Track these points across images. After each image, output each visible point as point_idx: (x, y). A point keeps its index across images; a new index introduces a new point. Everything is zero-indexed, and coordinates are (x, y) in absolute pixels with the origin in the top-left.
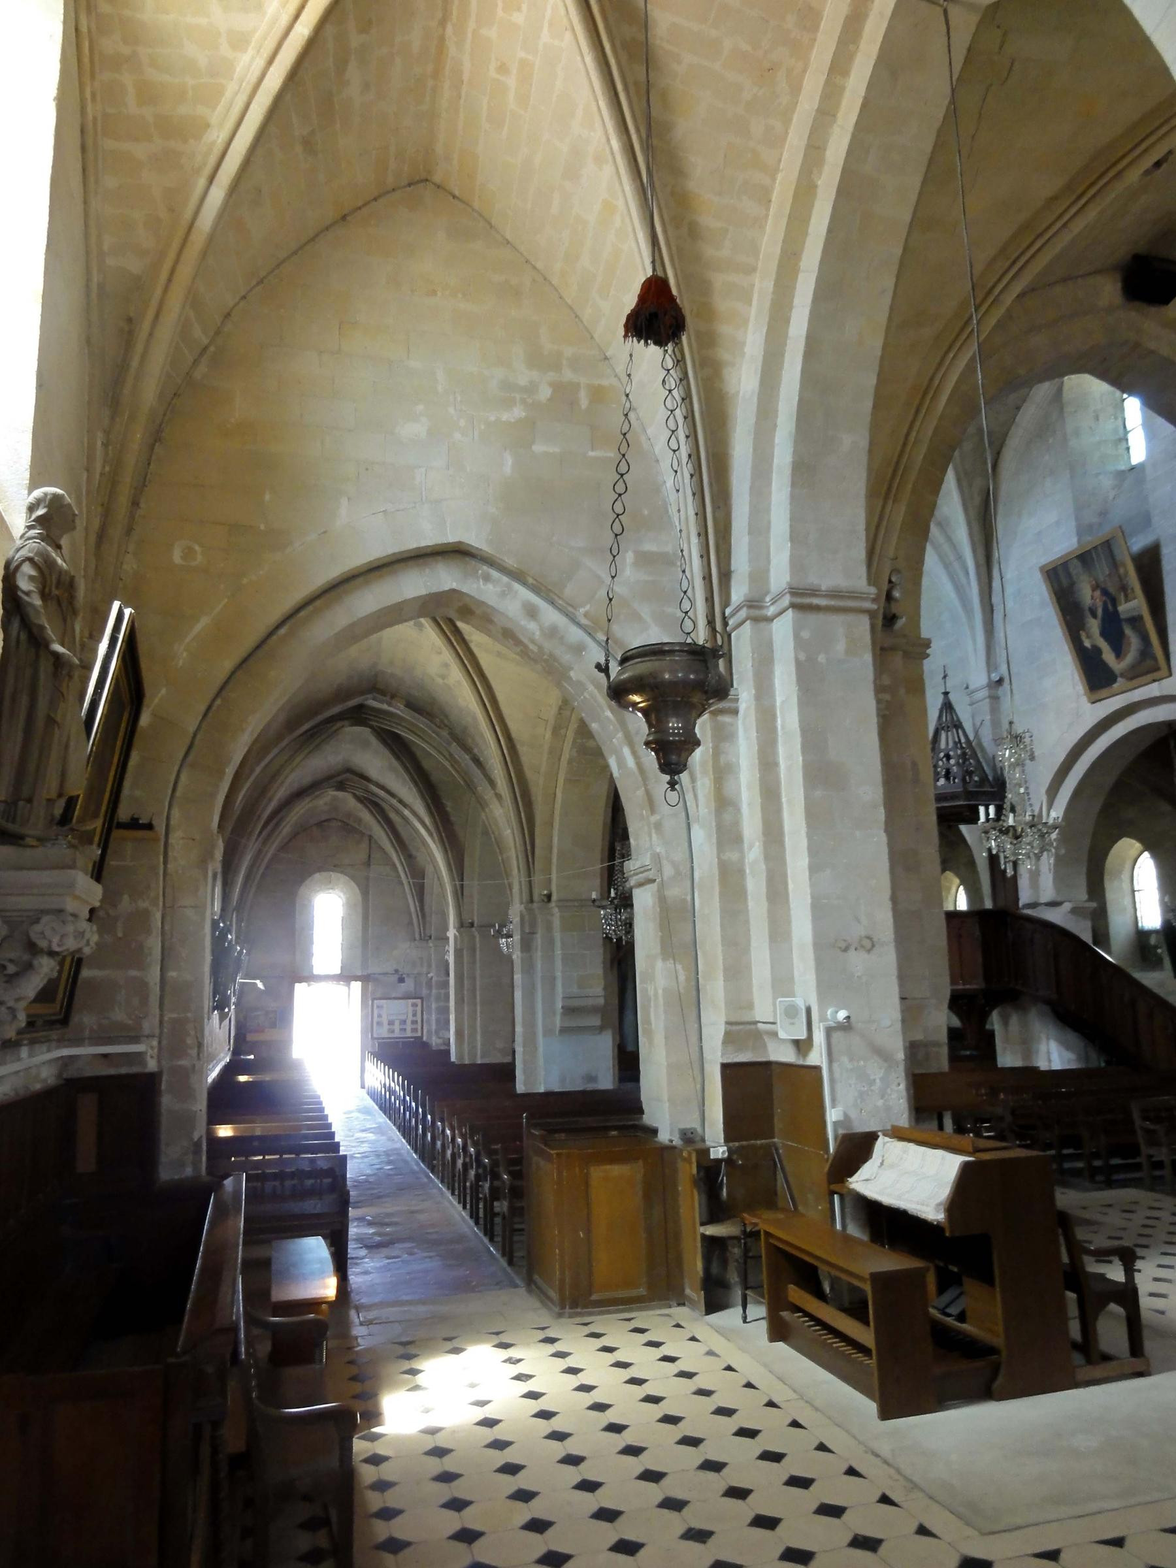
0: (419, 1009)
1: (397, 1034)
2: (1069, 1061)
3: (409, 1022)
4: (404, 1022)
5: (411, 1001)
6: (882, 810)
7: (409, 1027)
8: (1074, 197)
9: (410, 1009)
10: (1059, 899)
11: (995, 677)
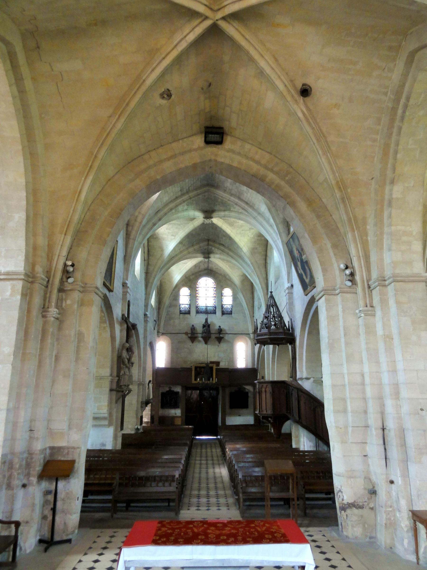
2: (310, 447)
6: (12, 357)
8: (117, 116)
10: (309, 377)
11: (289, 285)
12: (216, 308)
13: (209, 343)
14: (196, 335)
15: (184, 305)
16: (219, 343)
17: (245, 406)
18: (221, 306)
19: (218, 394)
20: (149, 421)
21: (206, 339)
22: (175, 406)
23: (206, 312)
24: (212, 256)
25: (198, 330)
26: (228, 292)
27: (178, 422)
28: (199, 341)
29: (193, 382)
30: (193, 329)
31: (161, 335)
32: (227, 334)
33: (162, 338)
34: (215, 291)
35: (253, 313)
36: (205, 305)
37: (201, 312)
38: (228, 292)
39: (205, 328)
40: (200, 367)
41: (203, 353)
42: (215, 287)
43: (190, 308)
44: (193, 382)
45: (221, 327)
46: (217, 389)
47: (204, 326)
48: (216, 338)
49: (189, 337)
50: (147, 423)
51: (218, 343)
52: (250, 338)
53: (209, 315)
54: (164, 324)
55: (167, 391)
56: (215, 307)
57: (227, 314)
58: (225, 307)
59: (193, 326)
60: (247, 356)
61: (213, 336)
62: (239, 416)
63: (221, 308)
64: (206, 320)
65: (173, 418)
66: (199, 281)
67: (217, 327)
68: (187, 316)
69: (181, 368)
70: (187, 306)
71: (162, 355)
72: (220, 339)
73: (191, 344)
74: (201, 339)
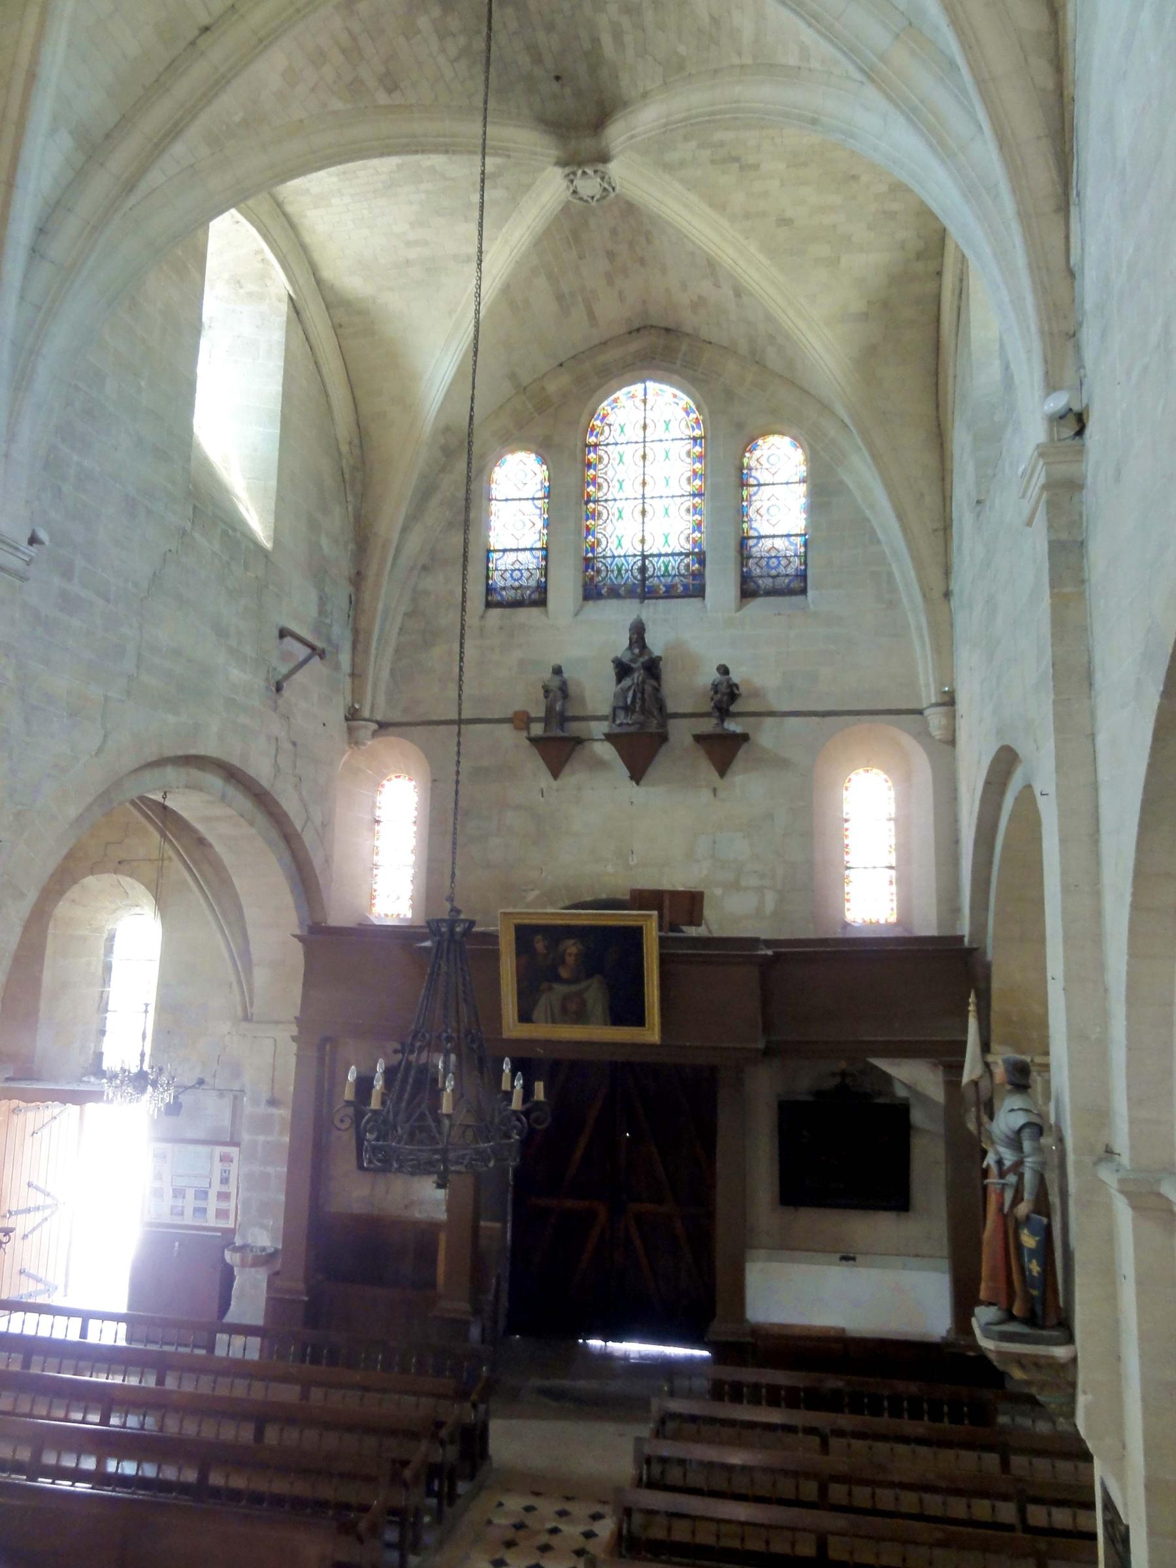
1: (188, 1219)
3: (212, 1195)
4: (202, 1194)
5: (219, 1150)
7: (213, 1204)
9: (218, 1167)
12: (702, 562)
13: (653, 772)
14: (574, 728)
15: (511, 557)
16: (722, 773)
17: (889, 1191)
18: (733, 544)
21: (640, 750)
23: (644, 587)
24: (617, 134)
26: (779, 462)
28: (600, 764)
29: (512, 1027)
31: (375, 734)
32: (771, 714)
33: (390, 747)
35: (947, 572)
37: (614, 593)
38: (779, 462)
39: (627, 682)
40: (556, 934)
41: (621, 835)
42: (698, 433)
44: (512, 1027)
45: (735, 677)
48: (699, 738)
49: (534, 741)
51: (715, 775)
52: (923, 735)
54: (392, 671)
56: (701, 558)
59: (558, 671)
60: (904, 849)
61: (681, 733)
62: (845, 1258)
63: (732, 553)
64: (638, 632)
67: (710, 675)
70: (530, 561)
73: (545, 779)
74: (606, 751)
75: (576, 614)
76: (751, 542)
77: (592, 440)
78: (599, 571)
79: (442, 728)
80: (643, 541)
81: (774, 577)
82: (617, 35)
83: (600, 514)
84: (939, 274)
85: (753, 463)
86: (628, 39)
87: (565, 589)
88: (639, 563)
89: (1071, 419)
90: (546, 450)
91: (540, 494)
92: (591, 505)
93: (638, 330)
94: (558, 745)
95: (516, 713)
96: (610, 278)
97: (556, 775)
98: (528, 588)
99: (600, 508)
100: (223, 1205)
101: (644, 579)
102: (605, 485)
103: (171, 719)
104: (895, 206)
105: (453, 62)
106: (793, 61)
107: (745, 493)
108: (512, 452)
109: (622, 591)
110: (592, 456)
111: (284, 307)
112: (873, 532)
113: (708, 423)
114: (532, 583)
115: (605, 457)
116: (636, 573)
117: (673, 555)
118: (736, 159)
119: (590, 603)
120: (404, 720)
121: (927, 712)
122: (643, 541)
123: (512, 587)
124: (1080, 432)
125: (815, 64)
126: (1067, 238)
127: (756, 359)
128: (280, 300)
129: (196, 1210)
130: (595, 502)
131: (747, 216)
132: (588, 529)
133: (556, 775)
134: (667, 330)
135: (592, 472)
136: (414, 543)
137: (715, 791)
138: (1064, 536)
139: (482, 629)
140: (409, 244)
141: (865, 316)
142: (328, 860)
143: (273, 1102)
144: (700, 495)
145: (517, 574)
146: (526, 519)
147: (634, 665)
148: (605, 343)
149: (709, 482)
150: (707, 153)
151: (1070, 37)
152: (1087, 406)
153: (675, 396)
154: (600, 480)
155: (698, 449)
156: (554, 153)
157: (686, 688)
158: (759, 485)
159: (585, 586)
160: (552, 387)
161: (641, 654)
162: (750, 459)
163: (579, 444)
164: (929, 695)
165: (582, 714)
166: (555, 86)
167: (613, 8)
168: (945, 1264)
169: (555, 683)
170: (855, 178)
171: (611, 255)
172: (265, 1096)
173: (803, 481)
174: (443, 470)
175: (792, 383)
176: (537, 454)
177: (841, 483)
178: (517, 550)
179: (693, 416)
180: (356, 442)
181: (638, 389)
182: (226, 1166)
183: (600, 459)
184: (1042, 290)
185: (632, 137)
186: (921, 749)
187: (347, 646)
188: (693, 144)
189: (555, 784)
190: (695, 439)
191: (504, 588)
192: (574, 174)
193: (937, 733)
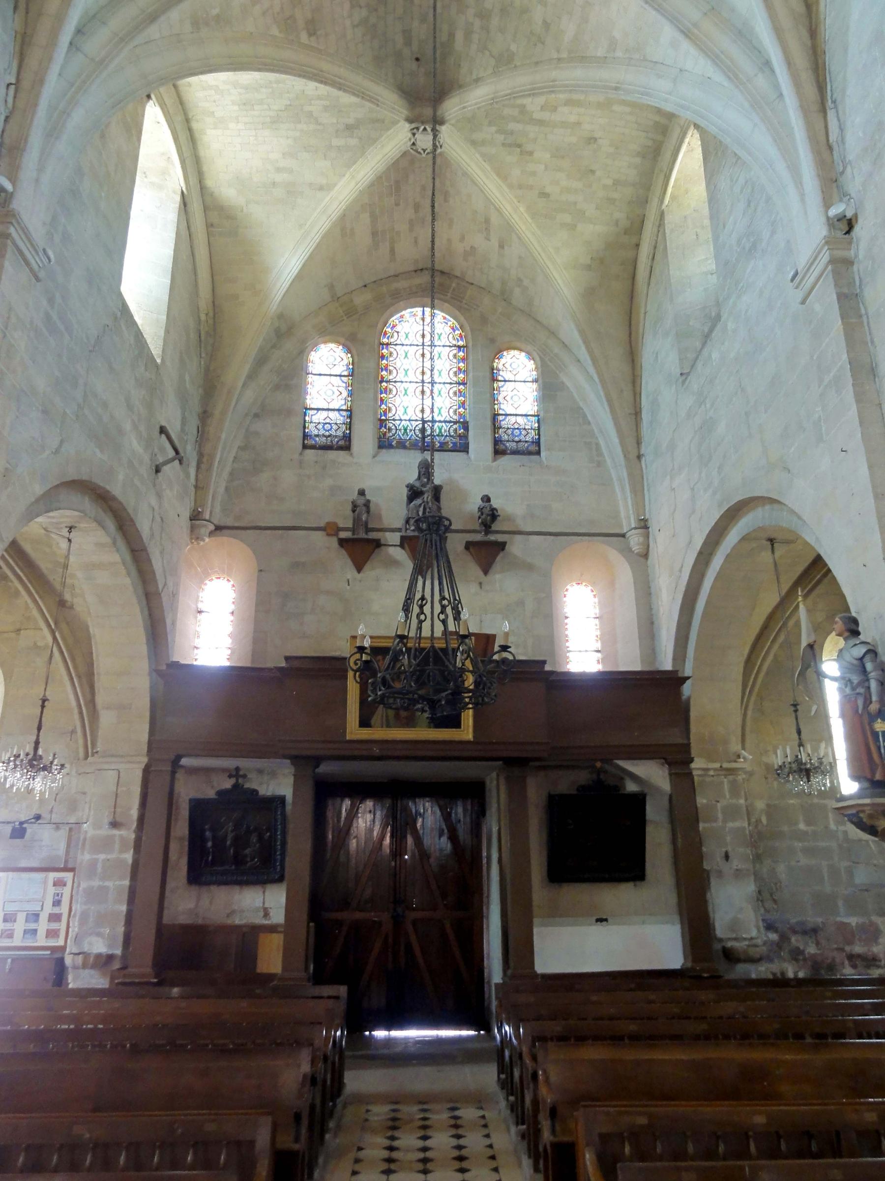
0: (67, 891)
5: (53, 876)
7: (43, 926)
9: (51, 890)
14: (373, 535)
16: (486, 572)
17: (628, 866)
19: (481, 812)
20: (118, 952)
22: (264, 869)
23: (425, 443)
24: (452, 108)
25: (384, 513)
27: (271, 959)
28: (394, 563)
29: (354, 730)
30: (362, 506)
31: (211, 534)
34: (463, 360)
35: (639, 443)
36: (414, 413)
37: (402, 445)
39: (418, 501)
42: (461, 343)
43: (350, 426)
44: (354, 730)
45: (495, 503)
46: (474, 792)
47: (414, 493)
48: (469, 546)
49: (342, 542)
50: (103, 962)
51: (481, 573)
52: (626, 551)
53: (436, 454)
55: (220, 793)
56: (465, 425)
57: (515, 452)
58: (507, 422)
59: (362, 493)
61: (455, 544)
62: (600, 920)
63: (489, 423)
64: (426, 470)
65: (249, 937)
66: (394, 319)
67: (474, 504)
68: (332, 455)
69: (287, 659)
70: (337, 418)
71: (214, 626)
72: (488, 550)
73: (350, 572)
74: (399, 554)
75: (374, 457)
76: (501, 418)
77: (385, 340)
78: (390, 429)
79: (269, 532)
80: (423, 411)
81: (517, 442)
82: (468, 34)
83: (391, 390)
84: (638, 245)
85: (500, 367)
86: (475, 37)
87: (364, 439)
88: (420, 426)
89: (845, 222)
90: (350, 343)
91: (346, 373)
92: (384, 384)
93: (422, 270)
94: (361, 546)
95: (328, 523)
96: (411, 223)
97: (359, 569)
98: (336, 436)
99: (391, 387)
100: (54, 926)
101: (424, 437)
102: (395, 372)
103: (99, 455)
104: (616, 195)
105: (354, 26)
106: (600, 53)
107: (495, 385)
108: (325, 342)
109: (407, 444)
110: (385, 351)
111: (178, 198)
112: (585, 416)
113: (470, 336)
114: (340, 433)
115: (395, 353)
116: (418, 433)
117: (445, 422)
118: (519, 146)
119: (384, 450)
120: (236, 525)
121: (628, 535)
122: (423, 411)
123: (324, 436)
124: (848, 232)
125: (619, 54)
126: (826, 127)
127: (505, 296)
128: (174, 192)
129: (26, 932)
130: (387, 382)
131: (520, 187)
132: (382, 400)
133: (359, 569)
134: (442, 273)
135: (384, 362)
136: (249, 395)
137: (480, 584)
138: (845, 290)
139: (301, 462)
140: (279, 170)
141: (589, 267)
142: (174, 623)
143: (114, 825)
144: (464, 384)
145: (327, 427)
146: (335, 389)
147: (424, 489)
148: (396, 276)
149: (471, 375)
150: (502, 137)
151: (822, 17)
152: (856, 216)
153: (445, 318)
154: (391, 368)
155: (461, 354)
156: (405, 112)
157: (462, 508)
158: (505, 381)
159: (380, 438)
160: (360, 299)
161: (428, 483)
162: (498, 364)
163: (376, 341)
164: (627, 521)
165: (377, 526)
166: (414, 65)
167: (471, 12)
168: (677, 918)
169: (361, 501)
170: (593, 172)
171: (417, 207)
172: (106, 820)
173: (536, 381)
174: (274, 346)
175: (529, 315)
176: (344, 346)
177: (563, 383)
178: (328, 410)
179: (457, 332)
180: (211, 314)
181: (419, 310)
182: (59, 890)
183: (391, 353)
184: (816, 152)
185: (464, 108)
186: (623, 559)
187: (194, 464)
188: (494, 129)
189: (359, 576)
190: (459, 347)
191: (317, 436)
192: (418, 129)
193: (636, 548)
